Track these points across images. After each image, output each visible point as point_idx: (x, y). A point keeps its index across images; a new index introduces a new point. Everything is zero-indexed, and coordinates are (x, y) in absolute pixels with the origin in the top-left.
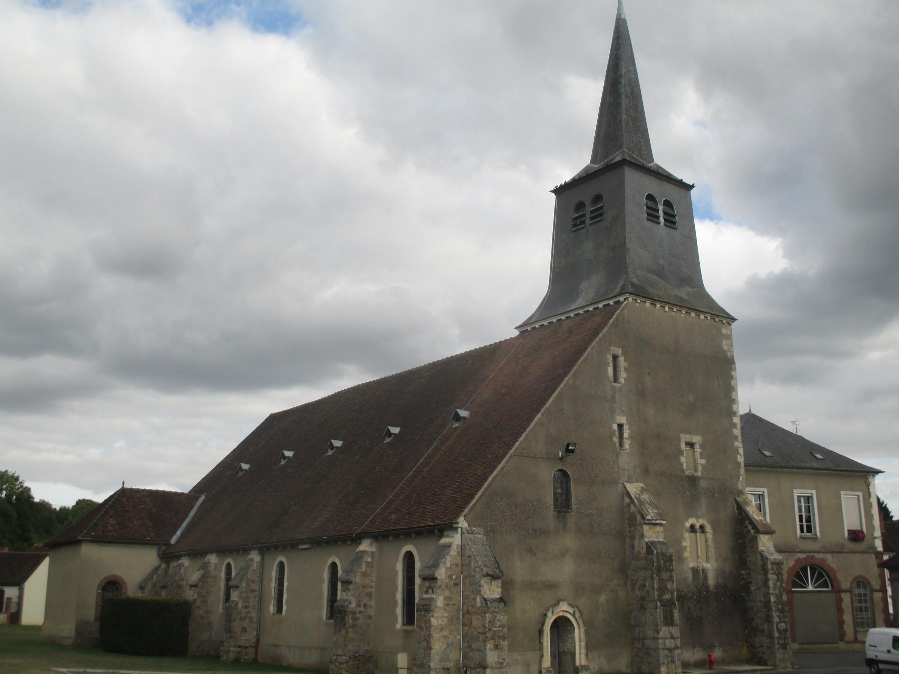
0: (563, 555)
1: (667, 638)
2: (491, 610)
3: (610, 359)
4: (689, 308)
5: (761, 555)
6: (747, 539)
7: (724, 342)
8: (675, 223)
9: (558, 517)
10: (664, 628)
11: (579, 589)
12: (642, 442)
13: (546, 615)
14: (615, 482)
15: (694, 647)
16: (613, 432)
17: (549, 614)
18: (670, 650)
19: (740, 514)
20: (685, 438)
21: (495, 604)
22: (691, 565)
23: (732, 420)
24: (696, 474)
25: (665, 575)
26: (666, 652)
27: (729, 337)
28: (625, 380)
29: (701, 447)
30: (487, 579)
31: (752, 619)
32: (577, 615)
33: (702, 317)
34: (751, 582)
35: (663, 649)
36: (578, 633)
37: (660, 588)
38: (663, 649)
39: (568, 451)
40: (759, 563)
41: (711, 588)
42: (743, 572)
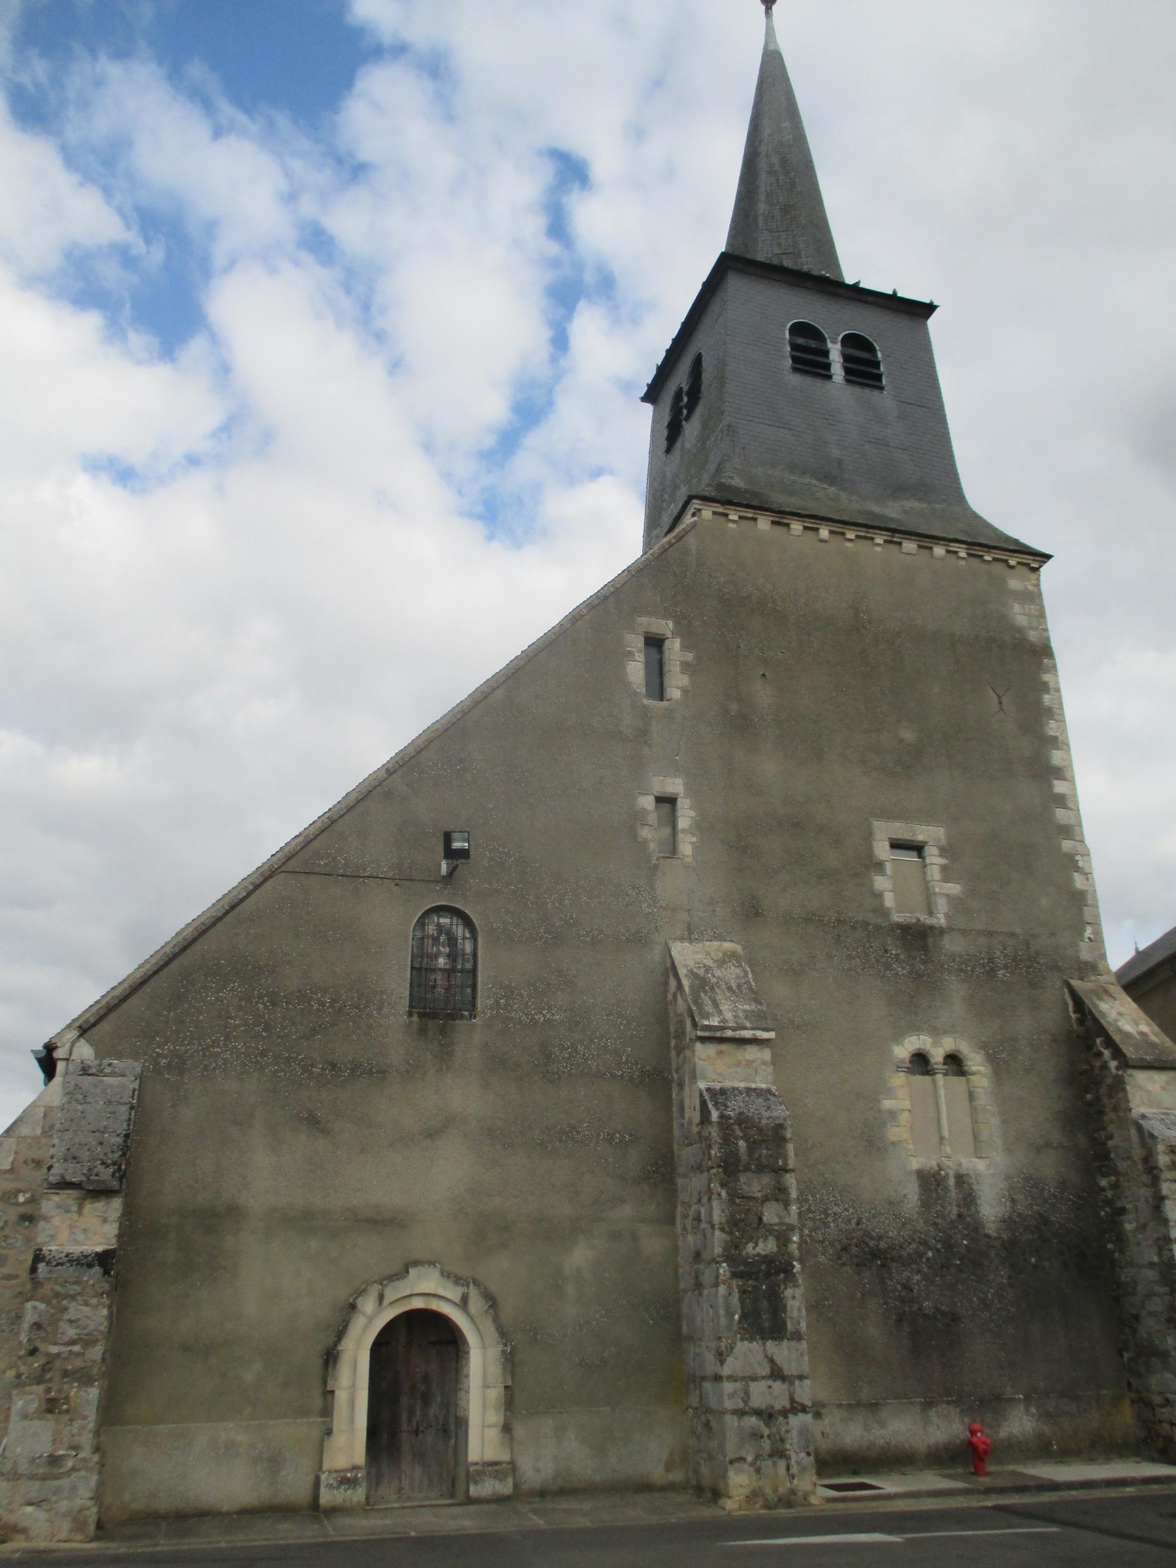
0: (431, 1135)
1: (754, 1379)
2: (46, 1290)
3: (636, 643)
4: (894, 531)
5: (1139, 1128)
6: (1103, 1090)
7: (1017, 608)
8: (878, 377)
9: (422, 1031)
10: (742, 1346)
11: (486, 1231)
12: (737, 841)
13: (353, 1307)
14: (639, 940)
15: (928, 1404)
16: (638, 817)
17: (368, 1305)
18: (768, 1415)
19: (1081, 1022)
20: (883, 832)
21: (70, 1271)
22: (915, 1164)
23: (1050, 786)
24: (929, 921)
25: (754, 1185)
26: (753, 1421)
27: (1034, 597)
28: (685, 691)
29: (943, 852)
30: (68, 1197)
31: (1137, 1317)
32: (477, 1304)
33: (939, 551)
34: (1123, 1211)
35: (740, 1413)
36: (481, 1365)
37: (732, 1224)
38: (740, 1413)
39: (451, 854)
40: (1138, 1153)
41: (991, 1229)
42: (1104, 1183)
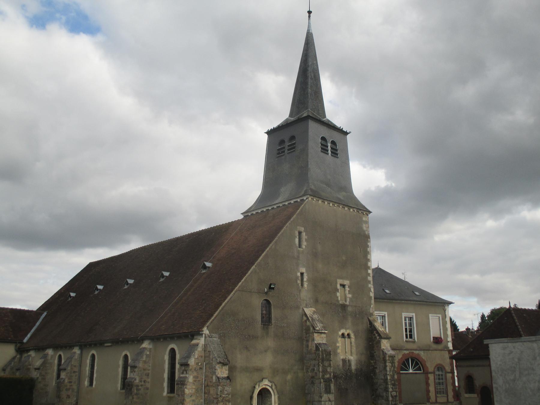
0: (266, 351)
2: (222, 384)
3: (297, 234)
5: (383, 351)
6: (375, 342)
8: (337, 154)
9: (264, 328)
10: (325, 395)
11: (275, 371)
12: (315, 283)
13: (255, 387)
14: (298, 307)
16: (297, 277)
17: (257, 387)
19: (371, 327)
20: (339, 281)
22: (342, 357)
24: (346, 303)
25: (326, 363)
27: (367, 222)
28: (306, 246)
29: (349, 287)
30: (220, 365)
31: (377, 389)
32: (274, 387)
33: (351, 210)
34: (376, 368)
37: (323, 371)
39: (270, 288)
40: (382, 356)
42: (372, 362)
